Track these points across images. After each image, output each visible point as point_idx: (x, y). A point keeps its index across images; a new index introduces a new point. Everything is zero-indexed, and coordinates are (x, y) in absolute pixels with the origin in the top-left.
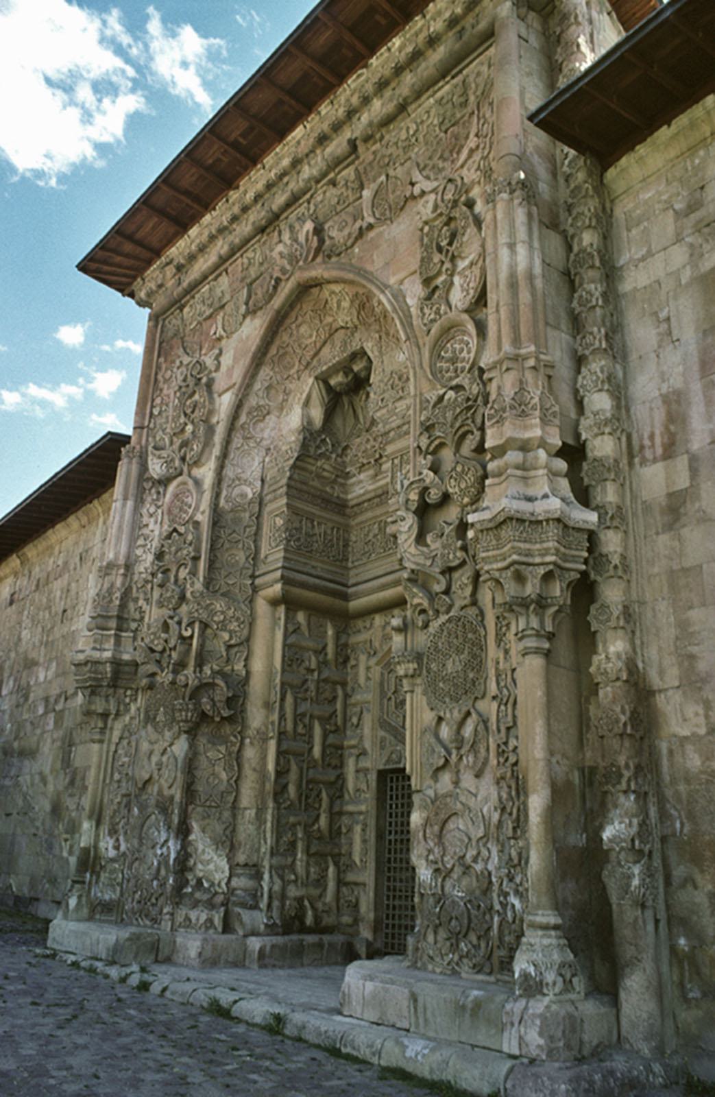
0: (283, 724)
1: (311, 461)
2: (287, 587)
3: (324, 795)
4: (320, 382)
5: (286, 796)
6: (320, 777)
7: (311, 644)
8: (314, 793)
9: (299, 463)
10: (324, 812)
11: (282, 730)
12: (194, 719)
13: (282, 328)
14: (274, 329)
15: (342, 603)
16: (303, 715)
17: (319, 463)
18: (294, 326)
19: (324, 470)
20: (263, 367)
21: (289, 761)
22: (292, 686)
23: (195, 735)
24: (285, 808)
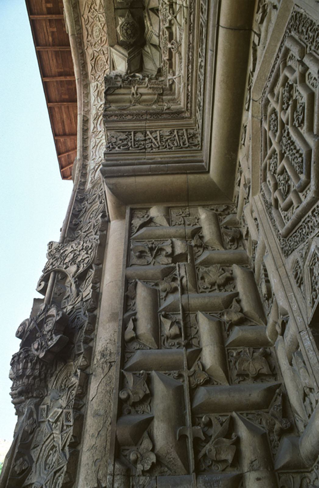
0: (131, 325)
1: (122, 91)
2: (113, 181)
3: (243, 432)
4: (117, 47)
5: (146, 444)
6: (222, 398)
7: (172, 230)
8: (216, 430)
9: (110, 97)
10: (252, 469)
11: (130, 334)
12: (28, 372)
13: (86, 48)
14: (80, 51)
15: (204, 177)
16: (173, 309)
17: (133, 90)
18: (89, 38)
19: (142, 94)
20: (91, 85)
21: (149, 381)
22: (145, 280)
23: (42, 398)
24: (144, 472)
